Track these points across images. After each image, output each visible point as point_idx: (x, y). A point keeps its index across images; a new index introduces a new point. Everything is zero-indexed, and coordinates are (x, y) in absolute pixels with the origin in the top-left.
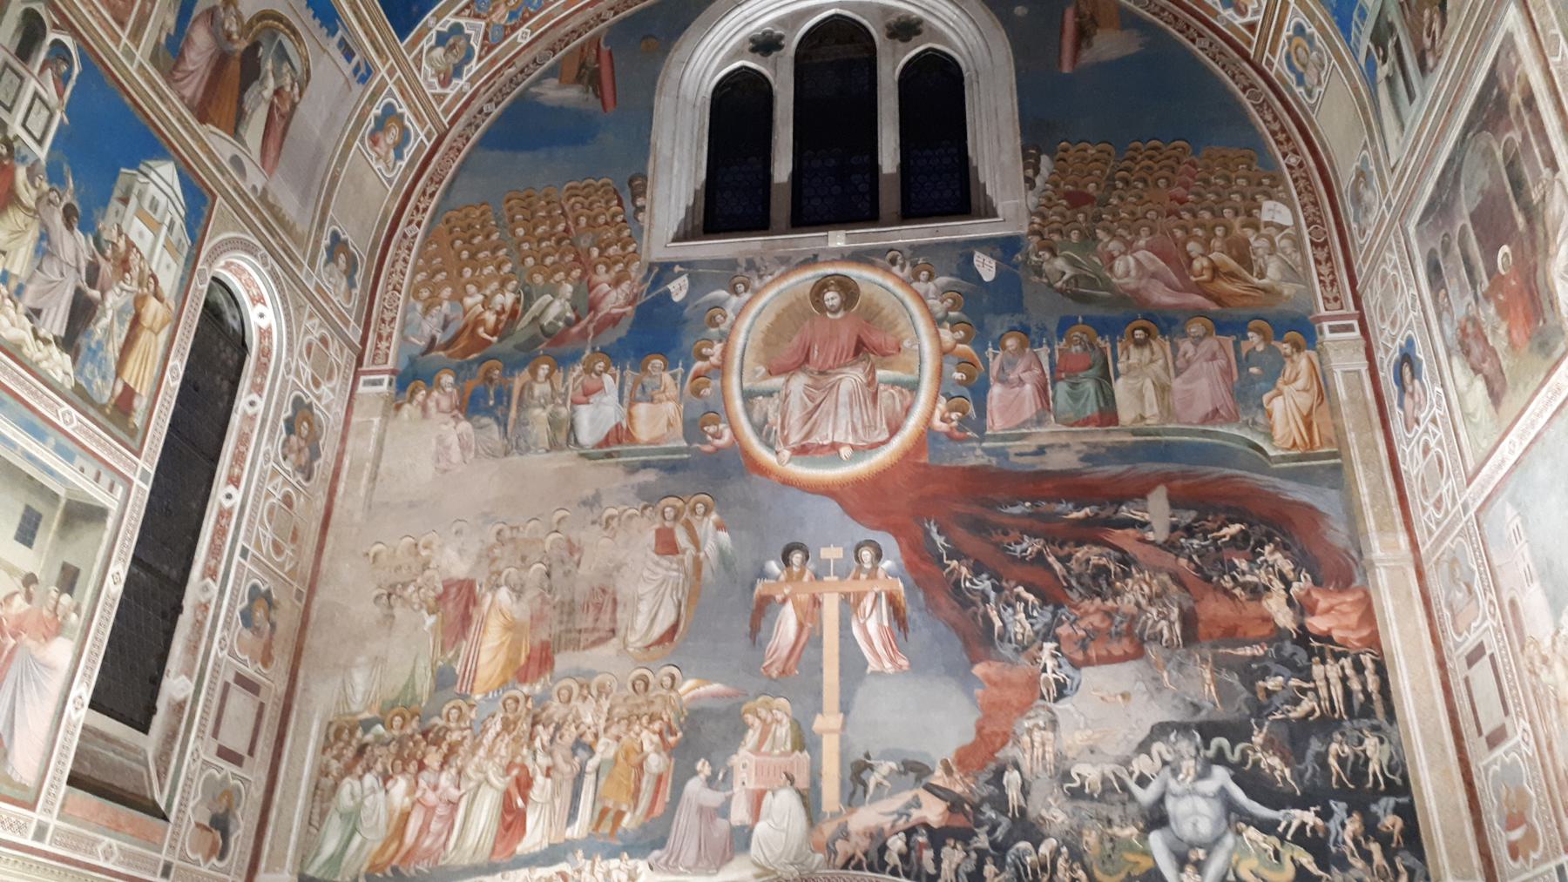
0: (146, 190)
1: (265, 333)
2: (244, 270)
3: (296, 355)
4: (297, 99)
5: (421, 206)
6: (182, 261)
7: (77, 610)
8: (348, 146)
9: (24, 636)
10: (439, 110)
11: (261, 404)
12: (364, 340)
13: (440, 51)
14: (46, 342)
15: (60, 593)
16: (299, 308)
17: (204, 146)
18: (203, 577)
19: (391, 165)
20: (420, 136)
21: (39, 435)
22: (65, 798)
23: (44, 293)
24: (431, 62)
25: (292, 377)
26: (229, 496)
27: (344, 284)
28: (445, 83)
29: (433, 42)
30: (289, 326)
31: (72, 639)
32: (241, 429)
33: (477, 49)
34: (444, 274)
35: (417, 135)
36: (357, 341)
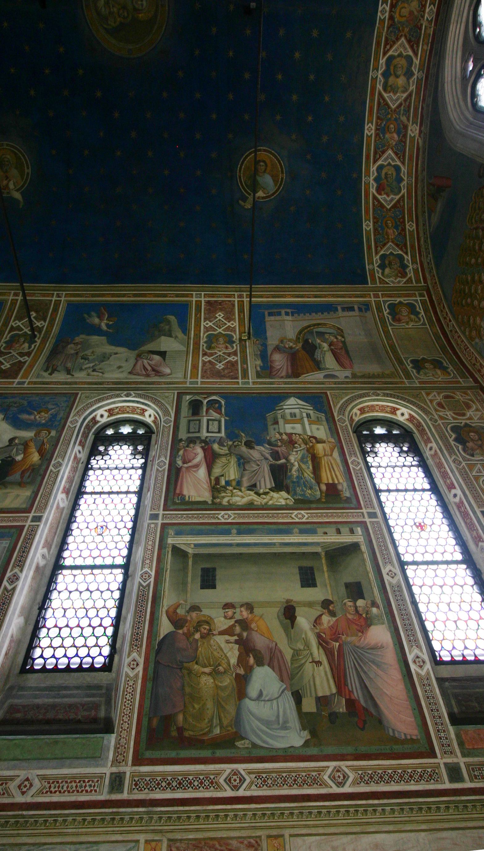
0: (285, 414)
1: (411, 419)
2: (372, 406)
3: (434, 413)
4: (343, 339)
5: (445, 316)
6: (325, 423)
7: (374, 604)
8: (387, 333)
9: (344, 637)
10: (415, 284)
11: (434, 445)
12: (476, 380)
13: (387, 271)
14: (266, 493)
15: (355, 601)
16: (416, 396)
17: (304, 383)
18: (477, 545)
19: (417, 319)
20: (417, 300)
21: (288, 532)
22: (458, 736)
23: (252, 477)
24: (388, 276)
25: (440, 422)
26: (455, 496)
27: (439, 372)
28: (404, 275)
29: (380, 271)
30: (417, 406)
31: (383, 623)
32: (435, 463)
33: (400, 252)
34: (471, 317)
35: (416, 301)
36: (473, 384)
